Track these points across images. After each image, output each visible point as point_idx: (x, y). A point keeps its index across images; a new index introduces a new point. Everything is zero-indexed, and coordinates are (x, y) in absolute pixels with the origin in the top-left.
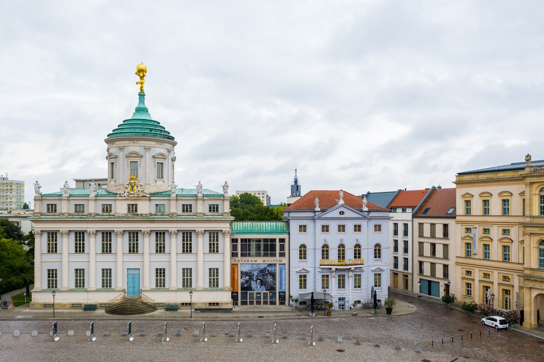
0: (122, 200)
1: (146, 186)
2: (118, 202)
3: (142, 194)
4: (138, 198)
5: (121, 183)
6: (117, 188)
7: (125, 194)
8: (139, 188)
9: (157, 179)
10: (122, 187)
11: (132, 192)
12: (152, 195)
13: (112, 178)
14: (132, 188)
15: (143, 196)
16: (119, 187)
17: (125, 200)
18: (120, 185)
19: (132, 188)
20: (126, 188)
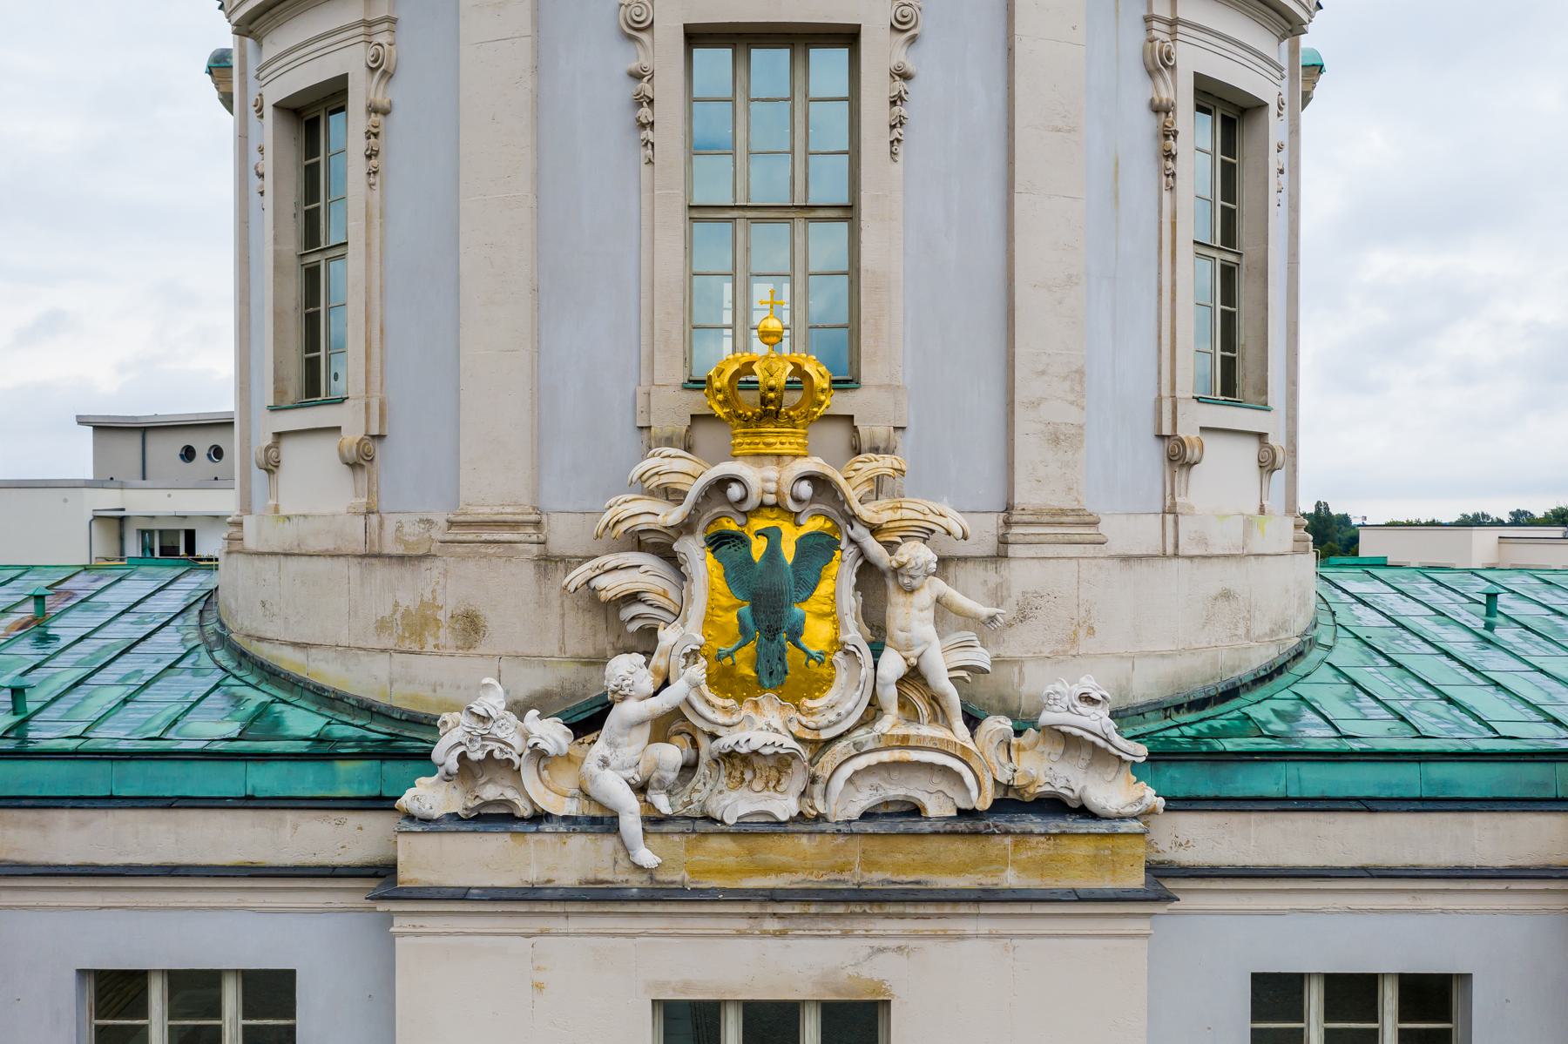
0: (530, 896)
1: (1023, 574)
2: (430, 954)
3: (994, 761)
4: (895, 865)
5: (492, 488)
6: (406, 591)
7: (615, 765)
8: (911, 617)
9: (1192, 420)
10: (504, 589)
11: (763, 725)
12: (1204, 743)
13: (312, 385)
14: (768, 608)
15: (1010, 803)
16: (450, 586)
17: (596, 896)
18: (477, 533)
19: (768, 608)
20: (623, 623)
